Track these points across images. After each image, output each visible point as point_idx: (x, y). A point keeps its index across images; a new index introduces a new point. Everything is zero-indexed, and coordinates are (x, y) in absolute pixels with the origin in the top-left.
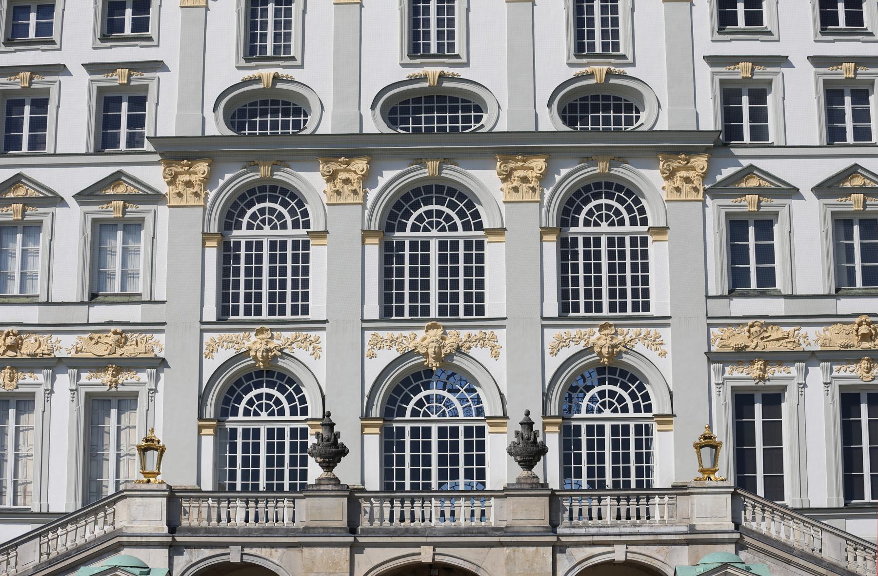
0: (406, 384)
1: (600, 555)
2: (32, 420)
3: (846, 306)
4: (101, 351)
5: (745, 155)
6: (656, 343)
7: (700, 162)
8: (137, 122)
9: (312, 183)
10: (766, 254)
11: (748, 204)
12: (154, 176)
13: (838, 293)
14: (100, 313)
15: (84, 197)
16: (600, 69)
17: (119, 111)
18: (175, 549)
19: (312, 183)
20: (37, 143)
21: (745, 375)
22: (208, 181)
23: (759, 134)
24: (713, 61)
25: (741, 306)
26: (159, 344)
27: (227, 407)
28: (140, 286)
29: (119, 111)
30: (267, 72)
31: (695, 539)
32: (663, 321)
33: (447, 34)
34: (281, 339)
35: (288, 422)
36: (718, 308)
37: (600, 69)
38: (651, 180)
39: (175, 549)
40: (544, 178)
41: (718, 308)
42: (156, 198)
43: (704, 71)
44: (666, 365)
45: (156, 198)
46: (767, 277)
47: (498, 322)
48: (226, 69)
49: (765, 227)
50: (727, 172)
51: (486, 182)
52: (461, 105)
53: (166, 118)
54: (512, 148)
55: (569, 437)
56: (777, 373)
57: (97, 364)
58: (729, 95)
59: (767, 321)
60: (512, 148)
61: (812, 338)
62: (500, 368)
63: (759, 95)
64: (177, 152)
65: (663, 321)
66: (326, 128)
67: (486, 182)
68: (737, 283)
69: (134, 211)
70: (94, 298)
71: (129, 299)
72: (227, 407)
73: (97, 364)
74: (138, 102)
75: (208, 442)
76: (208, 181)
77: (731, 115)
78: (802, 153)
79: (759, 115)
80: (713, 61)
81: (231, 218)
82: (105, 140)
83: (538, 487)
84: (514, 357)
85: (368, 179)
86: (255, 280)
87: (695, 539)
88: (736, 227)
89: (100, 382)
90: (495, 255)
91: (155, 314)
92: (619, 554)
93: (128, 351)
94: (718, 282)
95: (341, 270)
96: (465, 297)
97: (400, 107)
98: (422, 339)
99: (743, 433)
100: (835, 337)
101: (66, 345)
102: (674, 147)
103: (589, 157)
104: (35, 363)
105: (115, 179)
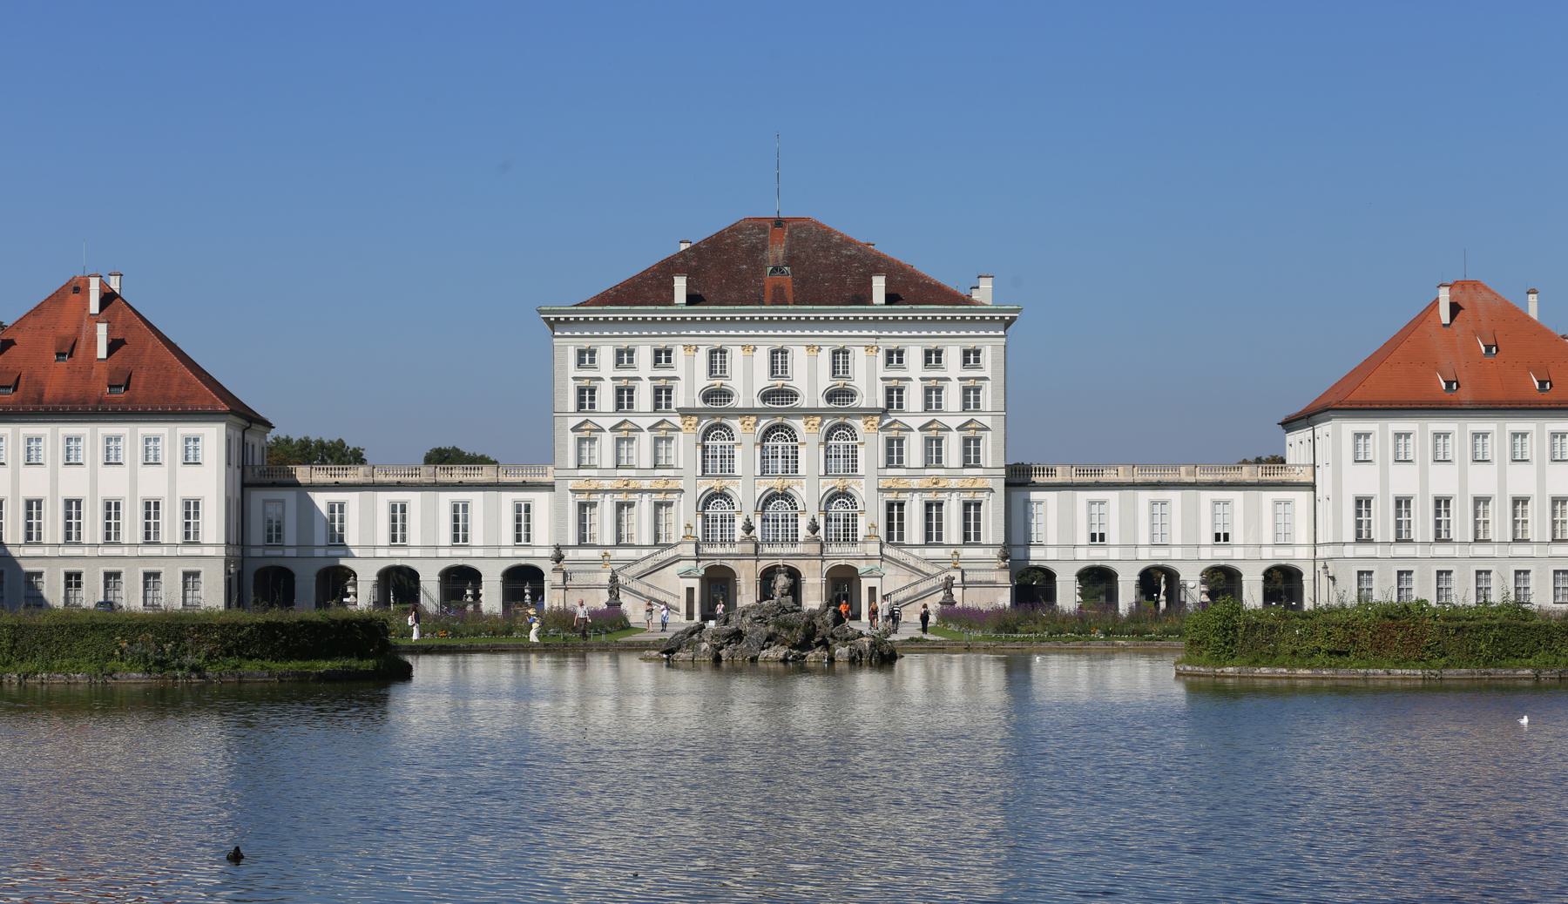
0: (770, 498)
1: (837, 563)
2: (634, 510)
3: (928, 472)
4: (660, 486)
5: (893, 416)
6: (859, 485)
7: (877, 419)
8: (668, 398)
9: (735, 424)
10: (900, 451)
11: (894, 434)
12: (677, 421)
13: (926, 467)
14: (658, 472)
15: (651, 428)
16: (841, 382)
17: (662, 395)
18: (698, 561)
19: (735, 424)
20: (630, 406)
21: (891, 497)
22: (698, 424)
23: (900, 406)
24: (883, 379)
25: (890, 472)
26: (681, 484)
27: (706, 506)
28: (672, 462)
29: (662, 395)
30: (718, 382)
31: (867, 558)
32: (862, 477)
33: (785, 367)
34: (726, 482)
35: (728, 512)
36: (882, 472)
37: (841, 382)
38: (859, 424)
39: (698, 561)
40: (820, 424)
41: (882, 472)
42: (679, 430)
43: (880, 383)
44: (863, 493)
45: (679, 430)
46: (900, 460)
47: (803, 477)
48: (703, 381)
49: (900, 441)
50: (887, 421)
51: (798, 424)
52: (789, 394)
53: (680, 399)
54: (808, 413)
55: (828, 520)
56: (902, 497)
57: (659, 491)
58: (889, 391)
59: (899, 477)
60: (808, 413)
61: (915, 483)
62: (803, 493)
63: (900, 391)
64: (685, 413)
65: (862, 477)
66: (740, 405)
67: (798, 424)
68: (889, 463)
69: (670, 434)
70: (656, 467)
71: (669, 467)
72: (706, 506)
73: (659, 491)
74: (669, 391)
75: (700, 519)
76: (698, 424)
77: (889, 399)
78: (915, 414)
79: (900, 399)
80: (883, 379)
81: (705, 436)
82: (657, 406)
83: (817, 540)
84: (808, 490)
85: (756, 424)
86: (713, 460)
87: (867, 558)
88: (890, 441)
89: (660, 497)
90: (802, 451)
91: (679, 473)
92: (843, 562)
93: (669, 487)
94: (882, 463)
95: (746, 457)
96: (792, 467)
97: (767, 396)
98: (776, 484)
99: (890, 517)
100: (925, 483)
101: (646, 484)
102: (867, 413)
103: (837, 416)
104: (635, 491)
105: (662, 422)
